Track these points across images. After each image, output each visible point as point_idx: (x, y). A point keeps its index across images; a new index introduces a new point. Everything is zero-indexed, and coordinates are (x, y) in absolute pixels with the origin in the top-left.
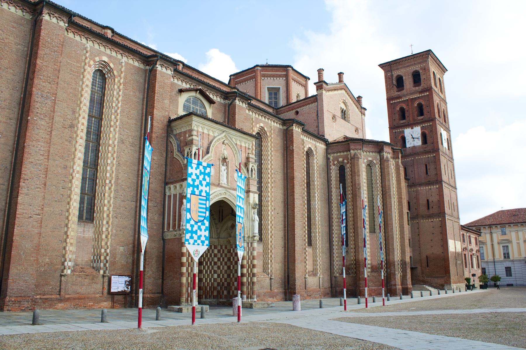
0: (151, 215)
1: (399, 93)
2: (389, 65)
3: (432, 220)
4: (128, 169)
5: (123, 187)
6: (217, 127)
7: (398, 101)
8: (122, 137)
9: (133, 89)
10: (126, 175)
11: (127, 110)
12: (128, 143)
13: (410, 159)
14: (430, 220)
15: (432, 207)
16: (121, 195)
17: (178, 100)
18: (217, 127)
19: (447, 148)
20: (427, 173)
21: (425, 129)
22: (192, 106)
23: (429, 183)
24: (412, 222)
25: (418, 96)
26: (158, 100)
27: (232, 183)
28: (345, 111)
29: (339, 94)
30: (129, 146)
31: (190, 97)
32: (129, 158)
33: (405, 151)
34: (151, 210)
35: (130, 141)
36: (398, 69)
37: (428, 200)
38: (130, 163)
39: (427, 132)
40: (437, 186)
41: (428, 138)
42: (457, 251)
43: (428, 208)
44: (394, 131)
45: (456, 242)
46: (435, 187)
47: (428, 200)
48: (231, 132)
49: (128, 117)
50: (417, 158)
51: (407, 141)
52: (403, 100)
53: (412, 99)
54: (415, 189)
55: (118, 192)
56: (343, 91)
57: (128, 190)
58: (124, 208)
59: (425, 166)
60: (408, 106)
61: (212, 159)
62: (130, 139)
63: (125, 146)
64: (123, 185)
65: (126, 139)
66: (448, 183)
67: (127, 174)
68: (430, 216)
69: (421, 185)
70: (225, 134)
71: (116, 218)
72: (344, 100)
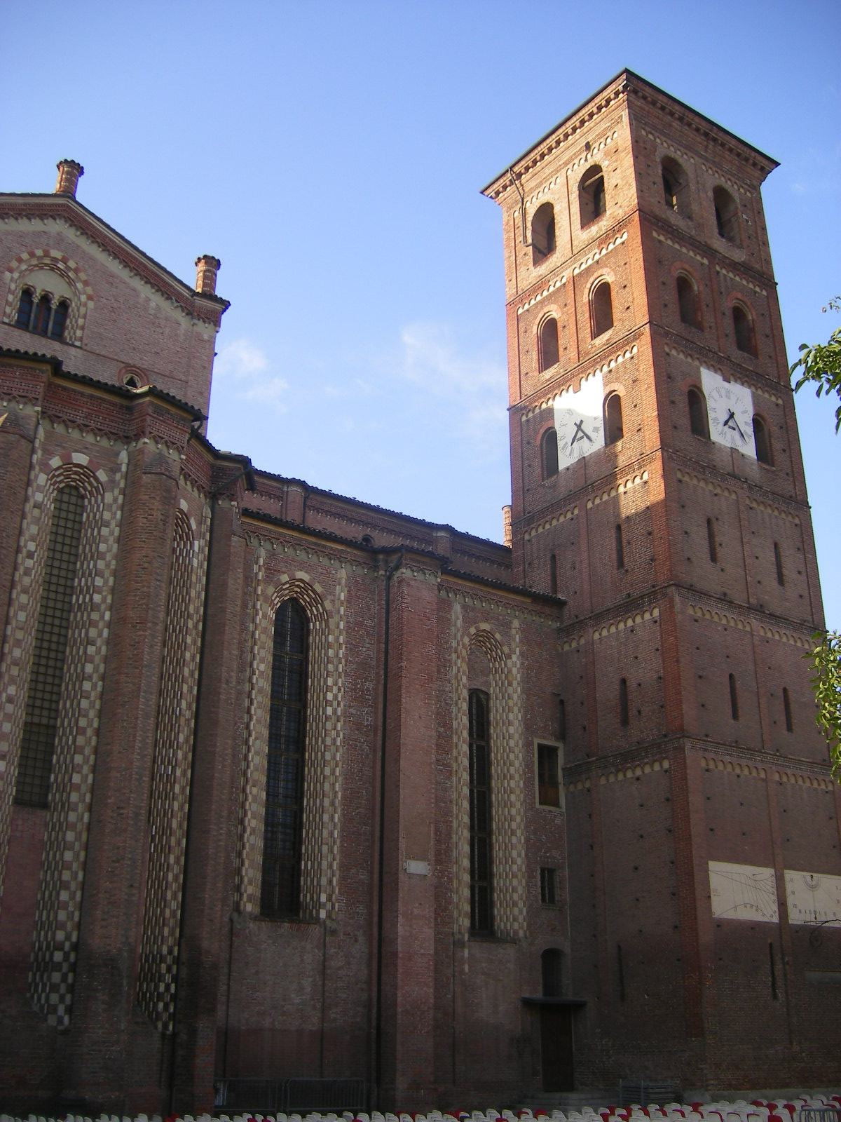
1: (543, 269)
2: (512, 182)
3: (638, 772)
7: (539, 298)
13: (569, 515)
14: (629, 774)
15: (639, 712)
19: (749, 449)
20: (621, 564)
21: (617, 380)
23: (630, 606)
24: (572, 788)
25: (597, 257)
28: (64, 305)
29: (8, 233)
33: (554, 487)
36: (541, 183)
37: (624, 681)
39: (621, 391)
40: (656, 612)
41: (626, 410)
42: (795, 918)
43: (625, 722)
44: (524, 418)
45: (789, 874)
46: (647, 616)
47: (624, 681)
50: (590, 505)
51: (560, 444)
52: (552, 289)
53: (580, 274)
54: (582, 641)
56: (57, 227)
59: (613, 533)
60: (565, 309)
66: (738, 597)
68: (628, 758)
69: (599, 618)
72: (55, 260)
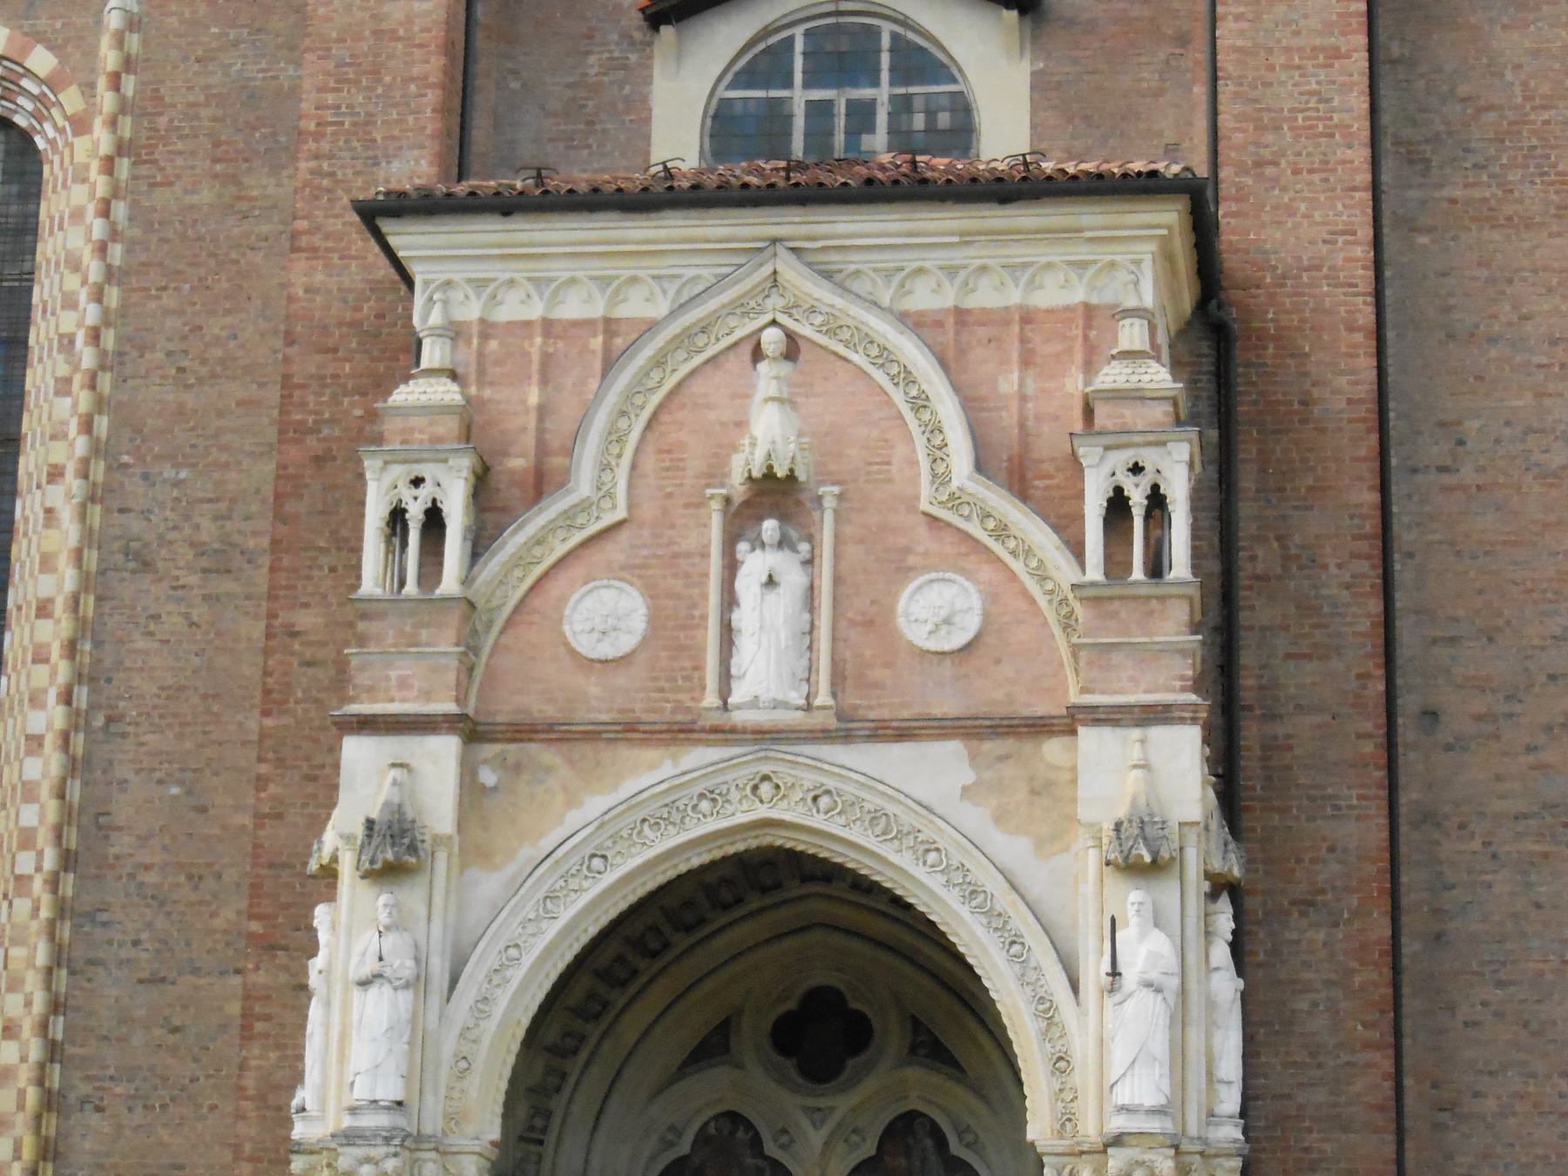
0: (273, 1055)
4: (188, 745)
5: (151, 878)
6: (662, 233)
8: (136, 525)
9: (217, 160)
10: (175, 790)
11: (171, 323)
12: (186, 554)
16: (136, 943)
17: (645, 100)
18: (662, 233)
22: (799, 97)
26: (325, 182)
27: (878, 674)
30: (193, 580)
31: (766, 32)
32: (196, 661)
34: (267, 1018)
35: (204, 537)
38: (205, 697)
48: (841, 228)
49: (181, 370)
55: (104, 924)
57: (193, 897)
58: (157, 1032)
61: (621, 513)
62: (206, 523)
63: (165, 585)
64: (147, 868)
65: (172, 535)
67: (181, 783)
70: (767, 270)
71: (99, 1109)
